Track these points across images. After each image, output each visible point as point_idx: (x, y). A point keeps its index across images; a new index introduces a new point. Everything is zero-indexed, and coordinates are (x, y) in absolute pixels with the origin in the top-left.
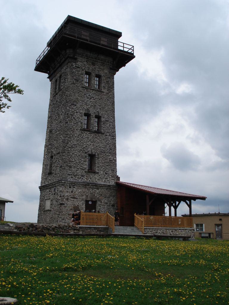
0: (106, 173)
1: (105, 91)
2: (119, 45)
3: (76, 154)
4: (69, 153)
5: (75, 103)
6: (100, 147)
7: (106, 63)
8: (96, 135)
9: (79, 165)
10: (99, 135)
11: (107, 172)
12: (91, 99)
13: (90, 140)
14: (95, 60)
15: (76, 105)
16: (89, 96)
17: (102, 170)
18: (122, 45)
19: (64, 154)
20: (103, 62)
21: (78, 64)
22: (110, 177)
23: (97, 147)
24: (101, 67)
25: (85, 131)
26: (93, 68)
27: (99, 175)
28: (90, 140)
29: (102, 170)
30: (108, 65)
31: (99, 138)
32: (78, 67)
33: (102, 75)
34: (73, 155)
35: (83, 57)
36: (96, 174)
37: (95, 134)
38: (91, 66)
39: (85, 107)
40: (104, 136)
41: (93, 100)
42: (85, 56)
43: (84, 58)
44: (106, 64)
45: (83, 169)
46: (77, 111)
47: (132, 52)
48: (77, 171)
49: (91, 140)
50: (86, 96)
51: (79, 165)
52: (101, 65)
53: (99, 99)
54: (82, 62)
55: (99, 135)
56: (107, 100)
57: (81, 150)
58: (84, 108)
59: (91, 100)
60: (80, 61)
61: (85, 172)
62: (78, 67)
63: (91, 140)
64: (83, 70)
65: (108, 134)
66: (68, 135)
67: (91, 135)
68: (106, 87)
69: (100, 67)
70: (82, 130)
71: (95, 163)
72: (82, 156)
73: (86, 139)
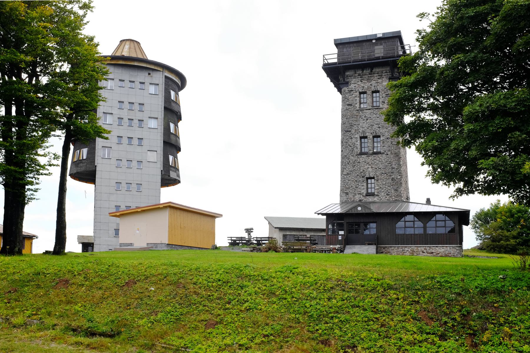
0: (387, 194)
4: (345, 180)
7: (384, 74)
11: (389, 192)
12: (367, 120)
14: (370, 76)
15: (350, 131)
16: (365, 117)
17: (383, 192)
22: (393, 197)
23: (376, 169)
24: (380, 81)
29: (383, 192)
30: (387, 75)
31: (378, 159)
32: (352, 91)
38: (367, 84)
39: (361, 131)
40: (384, 155)
41: (371, 121)
43: (358, 78)
44: (385, 75)
45: (360, 194)
48: (354, 196)
54: (355, 83)
57: (358, 175)
58: (359, 132)
59: (368, 121)
62: (352, 91)
64: (356, 92)
65: (389, 153)
70: (358, 155)
72: (359, 181)
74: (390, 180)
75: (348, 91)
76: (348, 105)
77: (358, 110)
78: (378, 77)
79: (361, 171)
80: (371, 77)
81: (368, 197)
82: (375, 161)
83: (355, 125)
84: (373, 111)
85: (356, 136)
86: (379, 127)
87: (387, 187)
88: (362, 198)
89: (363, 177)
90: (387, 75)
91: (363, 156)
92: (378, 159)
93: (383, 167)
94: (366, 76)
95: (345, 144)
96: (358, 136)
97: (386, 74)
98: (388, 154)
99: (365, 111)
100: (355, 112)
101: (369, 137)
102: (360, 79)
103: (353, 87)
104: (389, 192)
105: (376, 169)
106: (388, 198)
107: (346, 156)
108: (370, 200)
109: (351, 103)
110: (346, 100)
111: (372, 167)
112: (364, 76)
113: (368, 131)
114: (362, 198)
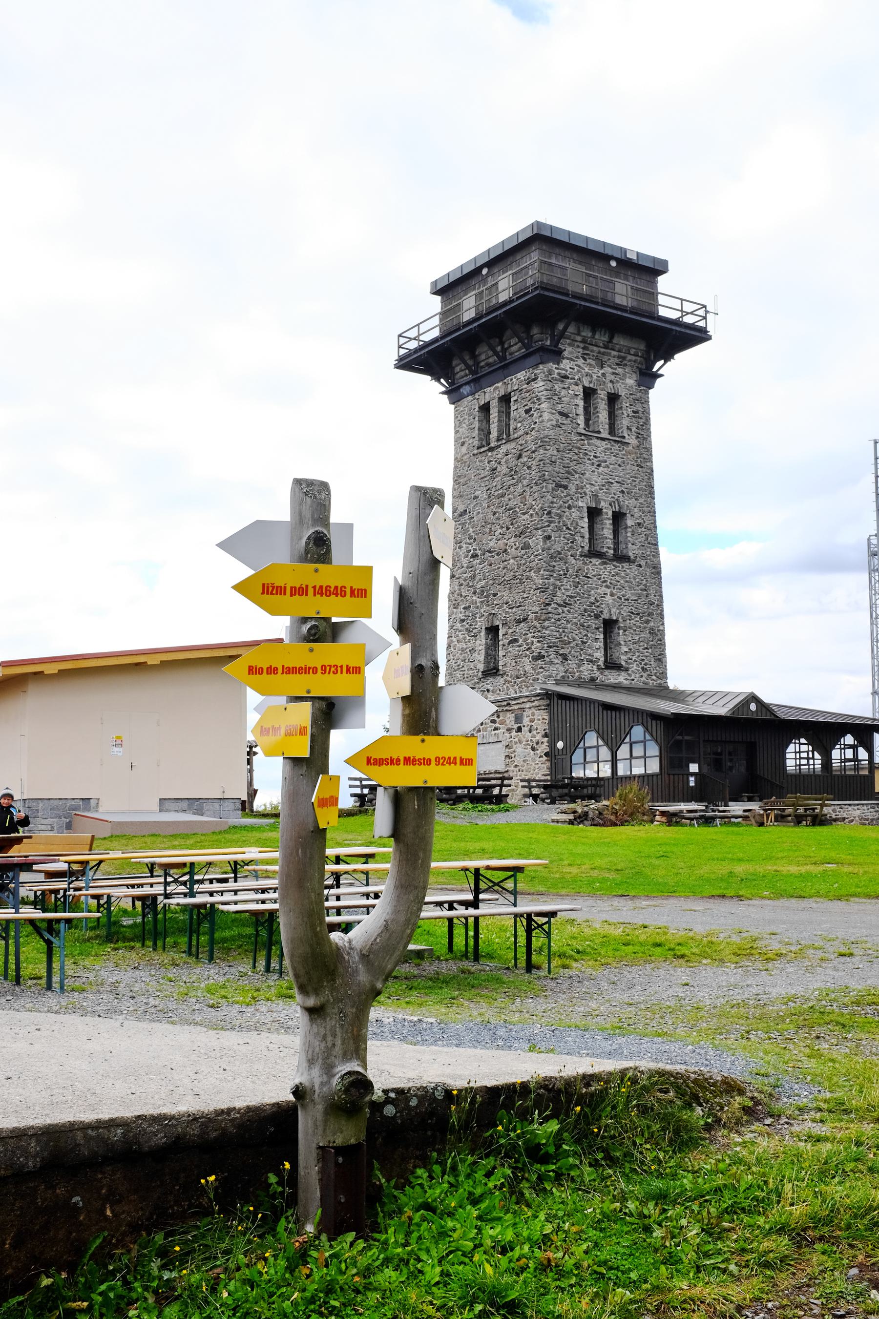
0: (643, 668)
1: (632, 441)
2: (660, 303)
3: (574, 620)
5: (564, 483)
6: (628, 600)
7: (629, 357)
8: (616, 567)
9: (582, 650)
10: (623, 567)
12: (599, 465)
13: (603, 582)
14: (602, 350)
15: (566, 487)
16: (595, 457)
17: (635, 661)
18: (677, 304)
19: (546, 623)
20: (623, 354)
21: (562, 366)
22: (654, 677)
24: (620, 370)
25: (590, 558)
26: (600, 375)
27: (630, 675)
28: (603, 582)
29: (635, 661)
31: (623, 574)
32: (566, 377)
33: (623, 394)
34: (569, 626)
35: (576, 344)
36: (623, 673)
37: (614, 563)
40: (634, 567)
41: (606, 470)
42: (581, 342)
43: (578, 347)
45: (591, 661)
46: (570, 502)
47: (702, 324)
48: (579, 666)
49: (605, 581)
50: (589, 459)
51: (582, 650)
52: (617, 364)
53: (619, 465)
54: (571, 360)
55: (623, 567)
56: (638, 465)
58: (586, 494)
59: (601, 469)
60: (568, 358)
61: (598, 667)
62: (566, 377)
63: (605, 581)
66: (553, 571)
67: (605, 568)
68: (634, 429)
69: (615, 369)
70: (585, 556)
71: (620, 644)
73: (595, 579)
74: (646, 635)
75: (559, 374)
76: (561, 414)
77: (580, 434)
78: (617, 360)
79: (592, 599)
80: (603, 354)
81: (607, 672)
82: (618, 578)
83: (576, 473)
84: (609, 446)
85: (581, 504)
86: (622, 492)
87: (641, 649)
88: (597, 674)
89: (597, 617)
90: (635, 361)
91: (594, 561)
92: (623, 574)
93: (633, 597)
94: (595, 348)
95: (556, 519)
96: (585, 505)
97: (634, 358)
98: (640, 566)
99: (594, 441)
100: (575, 438)
101: (607, 513)
102: (581, 350)
103: (568, 368)
104: (646, 664)
105: (620, 598)
106: (643, 679)
107: (559, 553)
108: (612, 681)
109: (566, 411)
110: (556, 398)
111: (612, 595)
112: (591, 347)
113: (601, 495)
114: (597, 674)
